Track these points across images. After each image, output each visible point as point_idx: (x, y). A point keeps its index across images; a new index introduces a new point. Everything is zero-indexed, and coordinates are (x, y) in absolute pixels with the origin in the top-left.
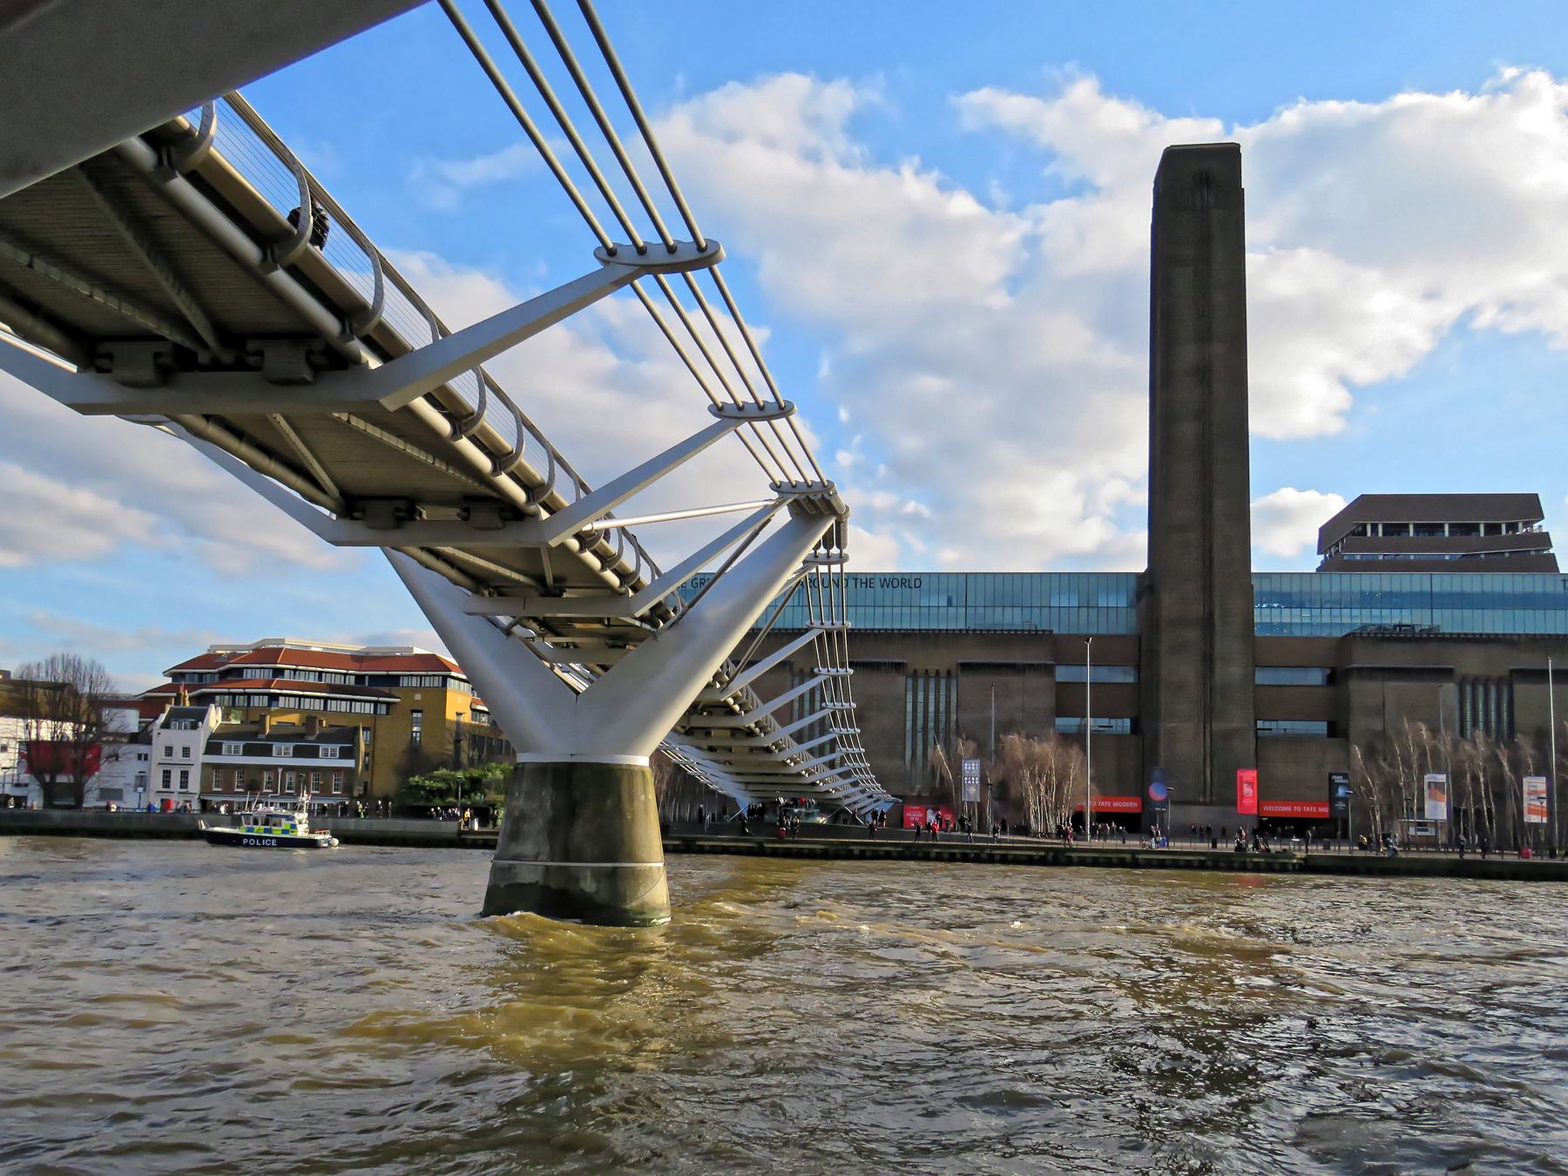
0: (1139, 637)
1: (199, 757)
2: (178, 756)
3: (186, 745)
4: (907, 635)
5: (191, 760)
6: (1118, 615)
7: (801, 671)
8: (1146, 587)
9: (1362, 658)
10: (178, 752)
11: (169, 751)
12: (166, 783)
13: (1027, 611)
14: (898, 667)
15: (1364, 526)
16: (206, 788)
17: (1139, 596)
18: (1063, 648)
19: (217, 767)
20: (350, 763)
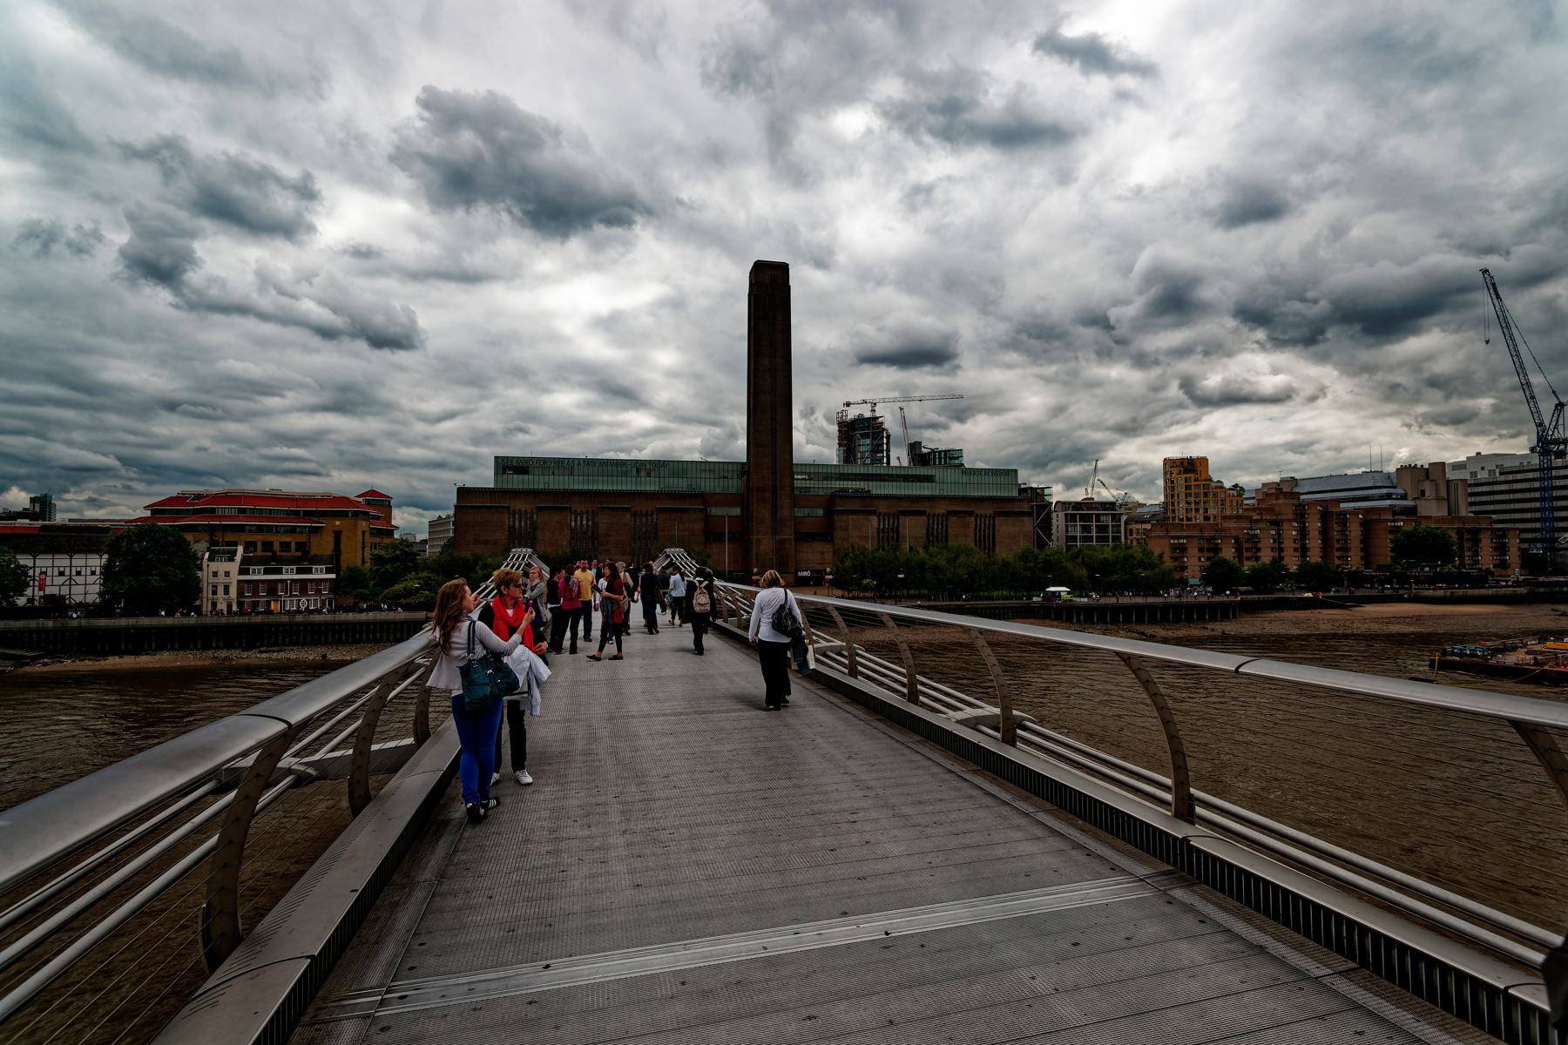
1: (235, 577)
3: (227, 570)
7: (576, 511)
8: (743, 470)
10: (221, 574)
12: (214, 593)
13: (690, 480)
14: (627, 509)
16: (240, 594)
17: (743, 474)
18: (704, 498)
20: (333, 576)
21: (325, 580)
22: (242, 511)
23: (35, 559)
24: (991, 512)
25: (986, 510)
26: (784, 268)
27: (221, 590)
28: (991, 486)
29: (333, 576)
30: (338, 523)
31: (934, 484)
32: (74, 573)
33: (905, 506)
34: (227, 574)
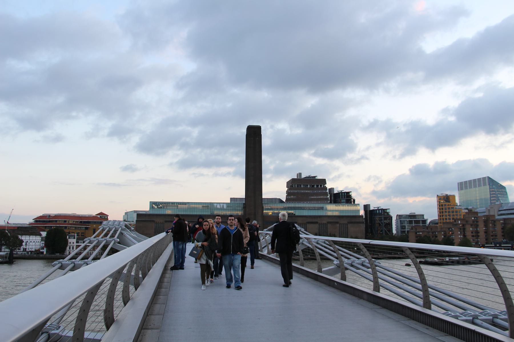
0: (243, 216)
1: (75, 244)
15: (293, 185)
22: (65, 221)
23: (22, 236)
24: (347, 222)
25: (345, 221)
26: (259, 128)
27: (71, 248)
30: (95, 226)
31: (323, 211)
32: (30, 242)
34: (73, 243)
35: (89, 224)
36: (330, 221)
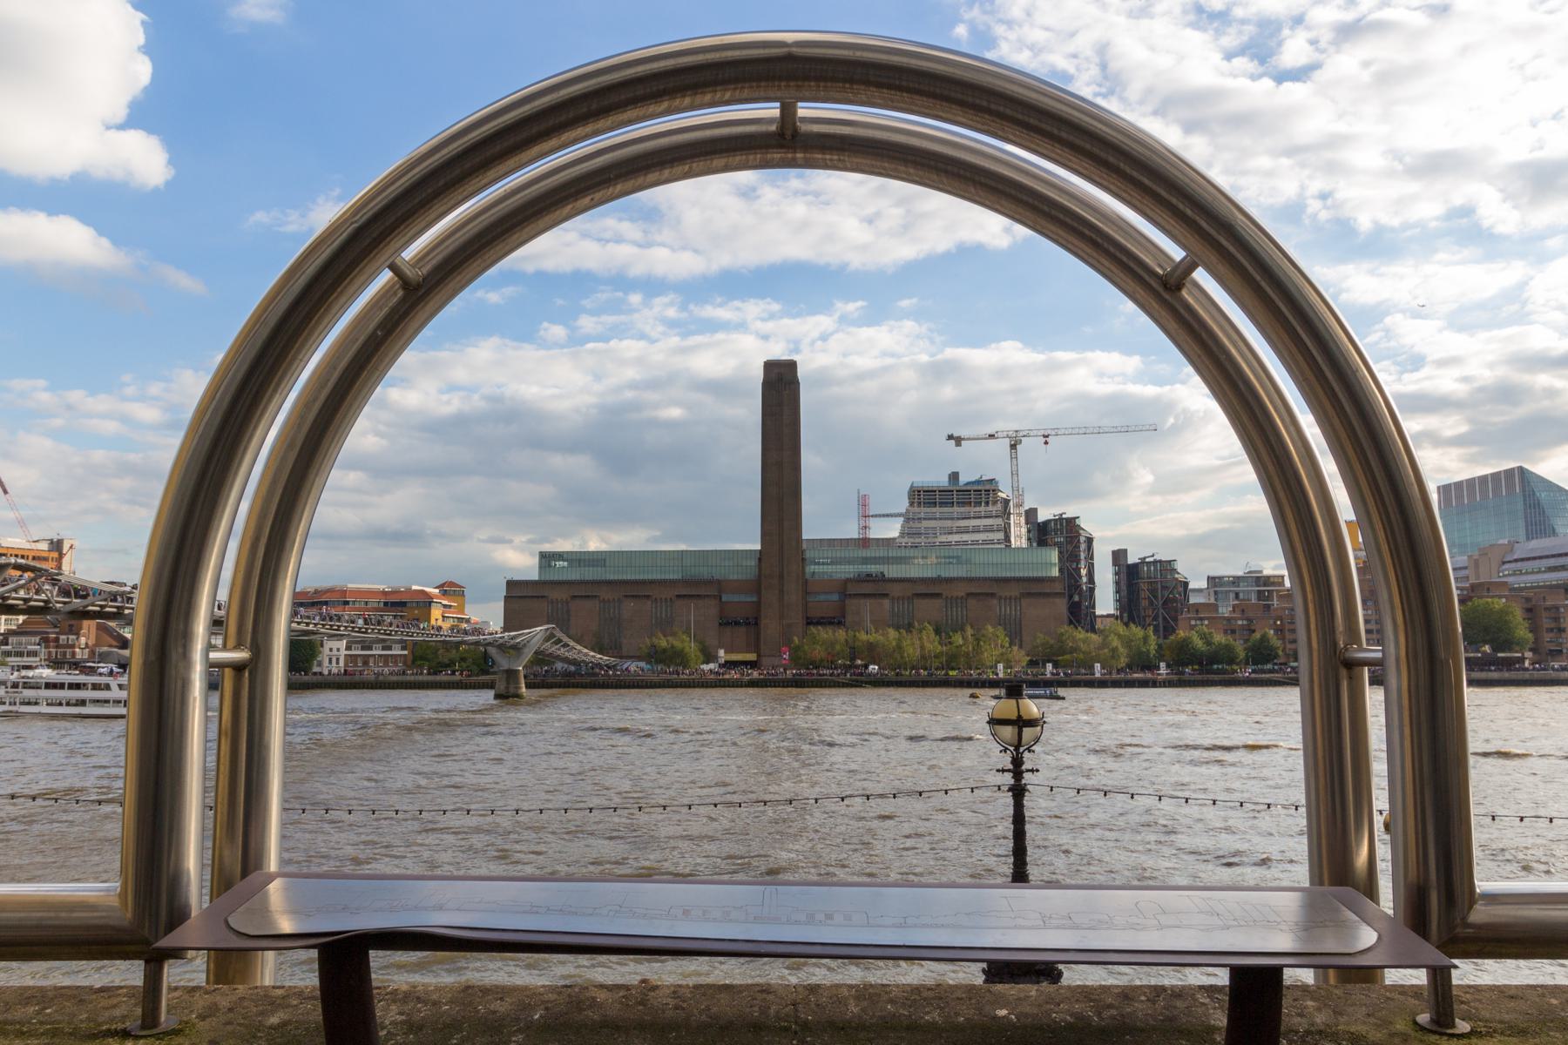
1: (344, 652)
2: (335, 652)
4: (652, 582)
5: (341, 653)
6: (749, 570)
8: (761, 556)
9: (852, 590)
10: (334, 650)
11: (331, 650)
14: (648, 597)
16: (346, 665)
19: (350, 656)
20: (406, 652)
21: (401, 655)
24: (1017, 594)
25: (1014, 591)
27: (334, 660)
28: (1021, 566)
29: (406, 652)
30: (416, 612)
33: (922, 589)
35: (404, 609)
36: (973, 590)
